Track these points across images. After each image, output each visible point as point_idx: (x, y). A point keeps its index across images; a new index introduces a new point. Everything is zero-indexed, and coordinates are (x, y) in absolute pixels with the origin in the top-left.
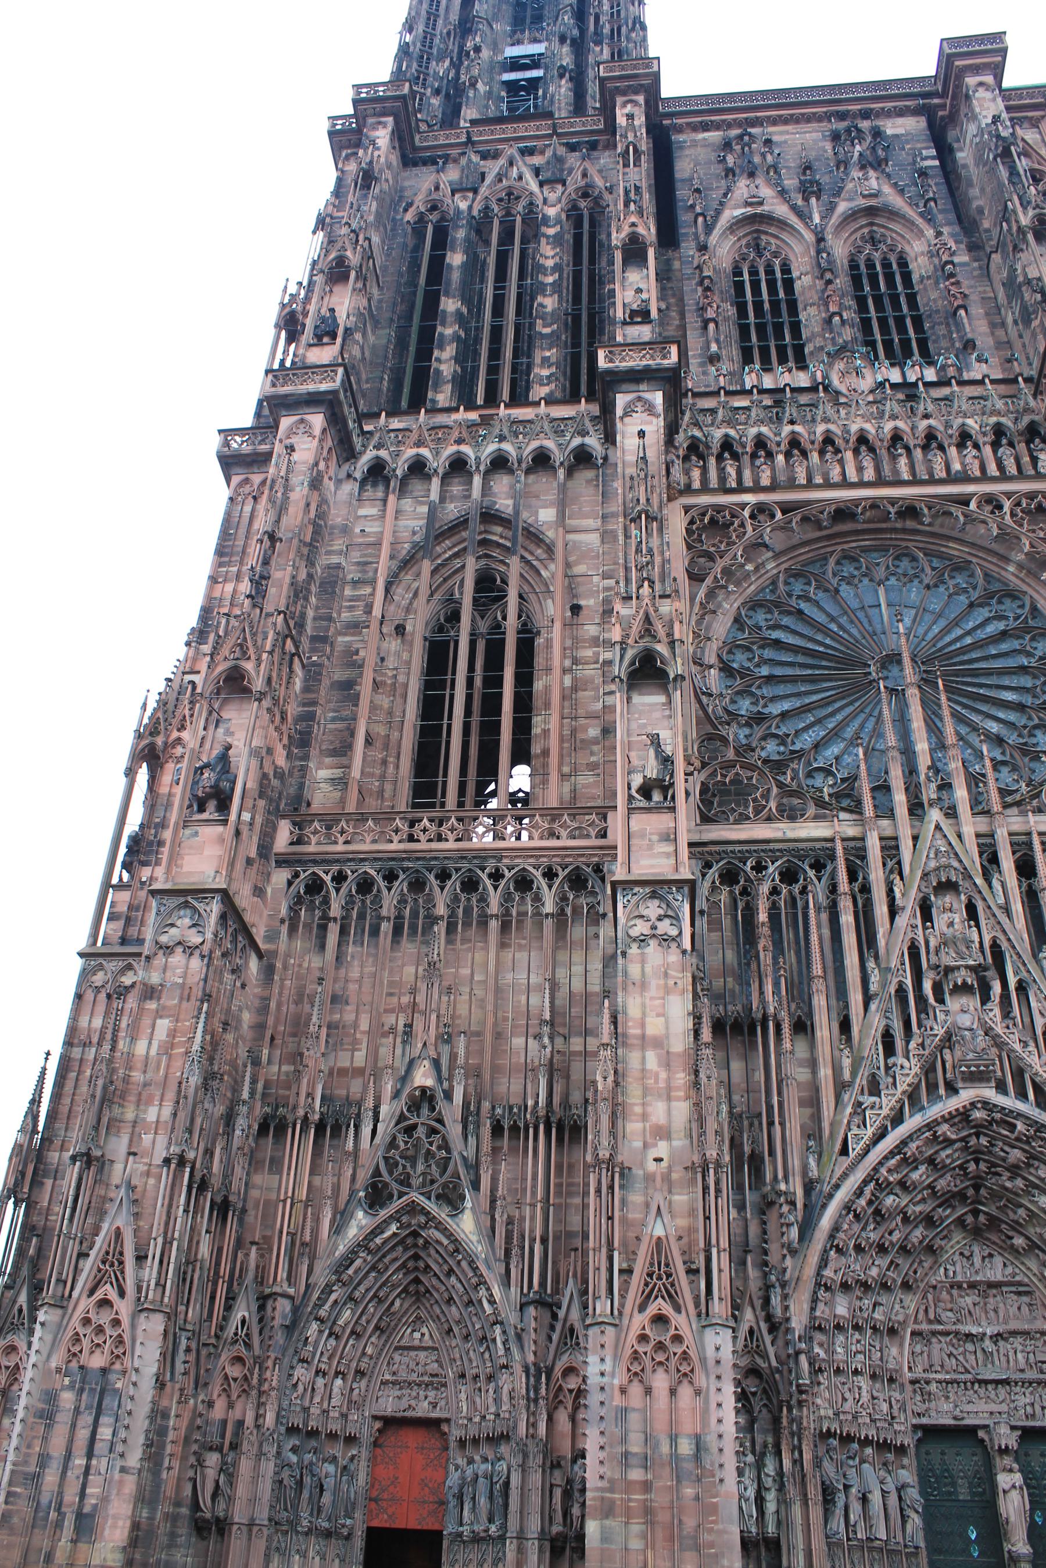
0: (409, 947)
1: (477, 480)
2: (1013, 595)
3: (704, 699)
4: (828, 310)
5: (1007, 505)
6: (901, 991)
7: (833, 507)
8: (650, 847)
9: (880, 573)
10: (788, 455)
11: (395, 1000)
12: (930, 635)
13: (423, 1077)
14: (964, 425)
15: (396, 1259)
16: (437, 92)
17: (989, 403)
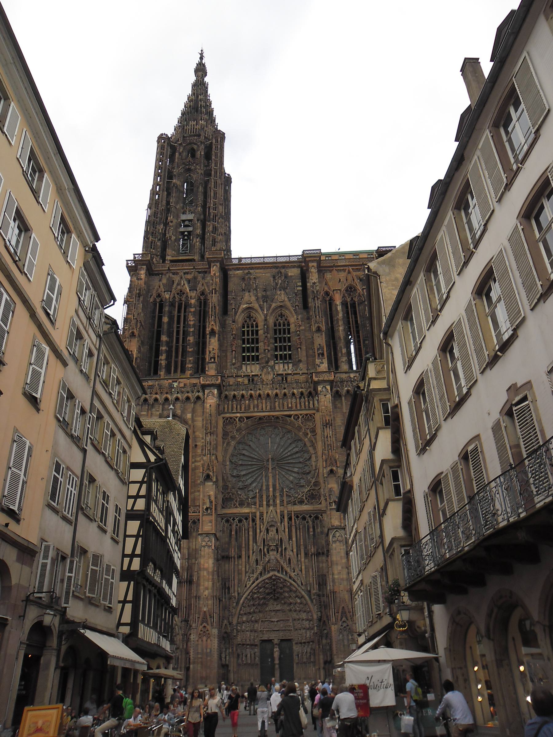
2: (301, 440)
5: (300, 417)
6: (261, 549)
10: (249, 400)
12: (280, 452)
16: (159, 240)
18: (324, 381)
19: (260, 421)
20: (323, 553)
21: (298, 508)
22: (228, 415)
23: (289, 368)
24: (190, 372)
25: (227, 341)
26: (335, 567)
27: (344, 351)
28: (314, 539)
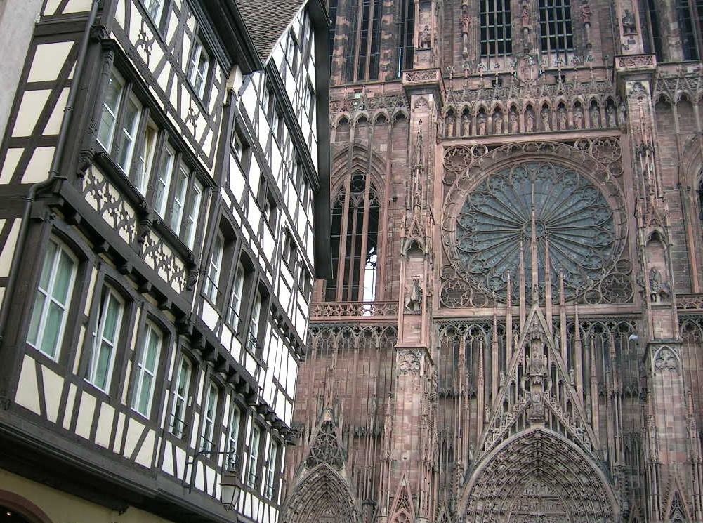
0: (323, 359)
1: (352, 131)
2: (592, 188)
3: (446, 247)
4: (522, 25)
5: (591, 144)
6: (513, 383)
7: (512, 146)
8: (411, 331)
9: (533, 176)
10: (494, 116)
11: (317, 382)
12: (553, 209)
13: (327, 417)
14: (577, 98)
15: (318, 486)
17: (590, 86)
18: (638, 73)
19: (516, 154)
20: (635, 395)
21: (586, 309)
22: (454, 143)
23: (571, 60)
24: (386, 74)
25: (453, 20)
26: (659, 417)
27: (673, 26)
28: (617, 367)
